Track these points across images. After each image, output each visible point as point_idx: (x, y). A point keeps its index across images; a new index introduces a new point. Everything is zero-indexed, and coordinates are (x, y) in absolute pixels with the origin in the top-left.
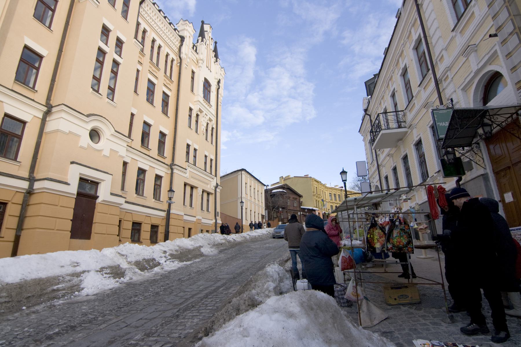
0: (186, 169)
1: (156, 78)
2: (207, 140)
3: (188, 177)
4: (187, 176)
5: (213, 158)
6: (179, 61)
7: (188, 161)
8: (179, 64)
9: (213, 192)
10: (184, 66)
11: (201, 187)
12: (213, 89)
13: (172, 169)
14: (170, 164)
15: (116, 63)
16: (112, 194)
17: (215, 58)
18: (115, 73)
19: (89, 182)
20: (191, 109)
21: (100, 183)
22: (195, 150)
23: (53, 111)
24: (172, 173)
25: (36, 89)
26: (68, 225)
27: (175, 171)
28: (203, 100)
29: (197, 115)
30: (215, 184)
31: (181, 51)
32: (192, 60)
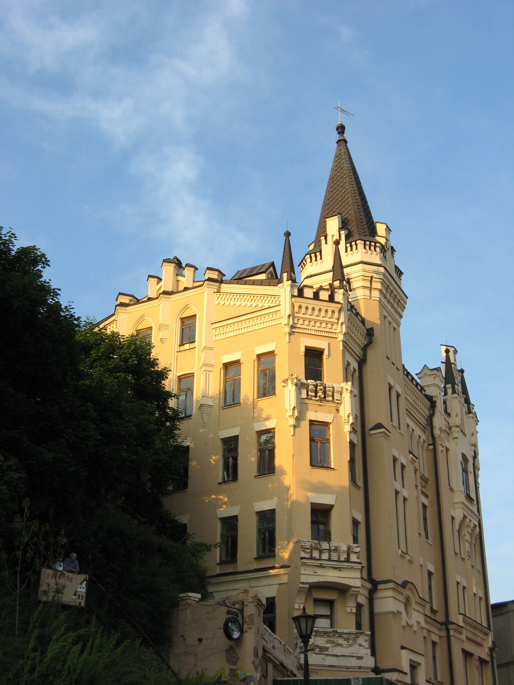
4: (463, 638)
5: (481, 594)
6: (431, 442)
8: (431, 447)
10: (440, 448)
13: (448, 630)
17: (466, 405)
21: (417, 667)
22: (464, 588)
23: (379, 588)
24: (448, 637)
27: (452, 633)
28: (465, 497)
29: (460, 524)
30: (490, 644)
31: (434, 425)
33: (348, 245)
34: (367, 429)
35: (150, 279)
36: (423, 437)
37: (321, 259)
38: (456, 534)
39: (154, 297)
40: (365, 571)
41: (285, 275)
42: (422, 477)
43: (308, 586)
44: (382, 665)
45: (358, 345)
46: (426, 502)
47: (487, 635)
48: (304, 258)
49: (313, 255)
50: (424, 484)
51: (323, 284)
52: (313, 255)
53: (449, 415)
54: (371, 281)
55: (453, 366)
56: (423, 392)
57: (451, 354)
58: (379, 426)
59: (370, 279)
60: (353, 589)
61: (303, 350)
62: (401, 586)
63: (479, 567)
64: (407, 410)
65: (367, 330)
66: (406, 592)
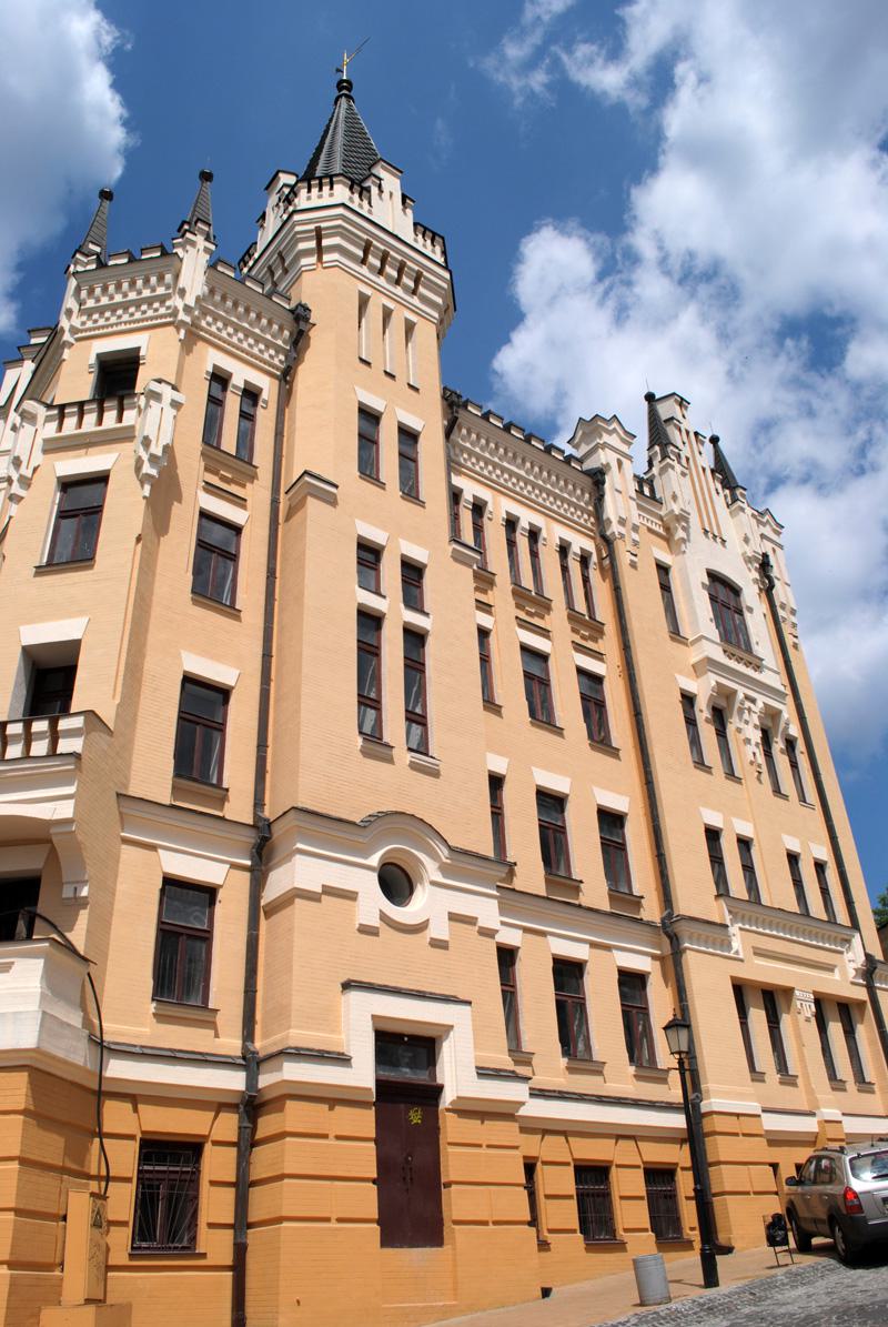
1: (545, 633)
2: (777, 791)
3: (741, 956)
4: (737, 952)
5: (824, 853)
8: (607, 562)
9: (861, 994)
10: (624, 558)
11: (804, 983)
12: (751, 595)
13: (674, 939)
14: (663, 920)
16: (484, 1073)
17: (727, 492)
18: (415, 667)
19: (406, 1039)
20: (688, 700)
22: (744, 844)
25: (225, 785)
26: (367, 1200)
28: (725, 651)
32: (650, 530)
36: (580, 543)
38: (707, 732)
47: (848, 941)
54: (319, 237)
61: (93, 360)
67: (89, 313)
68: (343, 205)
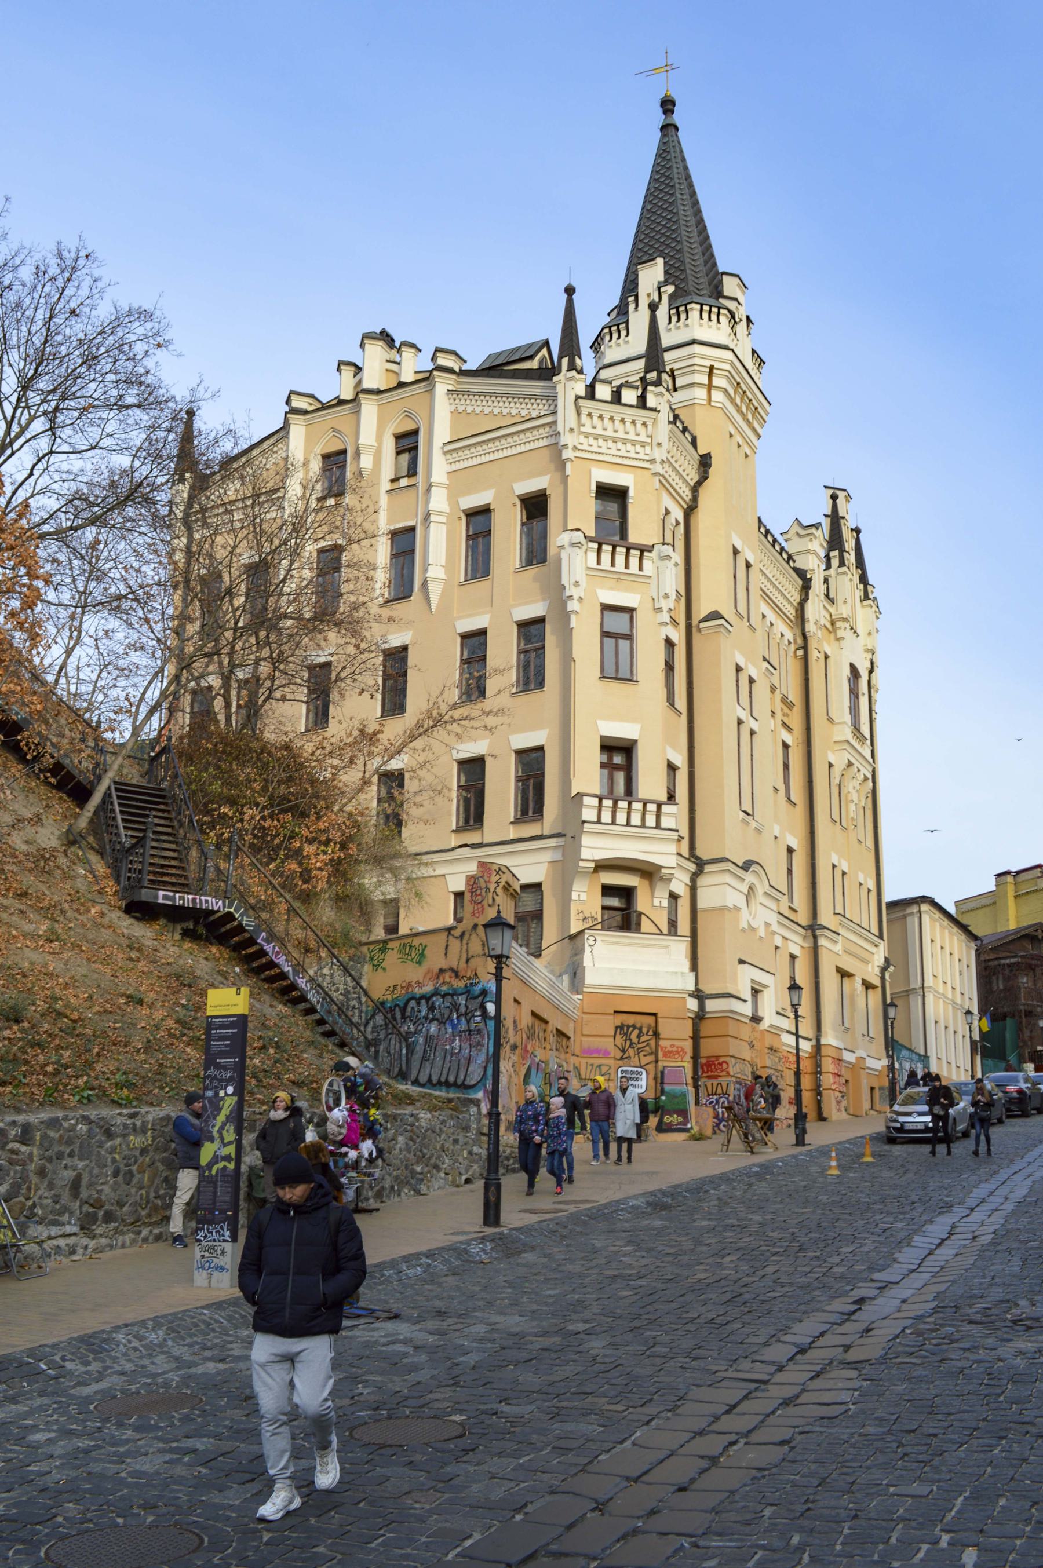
0: (838, 934)
5: (871, 884)
6: (800, 641)
7: (835, 914)
8: (800, 653)
10: (814, 655)
15: (752, 733)
17: (861, 586)
20: (831, 765)
24: (815, 950)
27: (822, 942)
33: (673, 311)
34: (695, 622)
35: (342, 367)
36: (789, 635)
37: (628, 335)
38: (835, 791)
39: (349, 398)
40: (685, 844)
41: (565, 361)
42: (784, 700)
43: (592, 865)
44: (707, 988)
45: (685, 481)
46: (789, 740)
48: (599, 334)
49: (614, 328)
50: (786, 710)
51: (631, 379)
52: (614, 328)
53: (832, 601)
55: (842, 521)
56: (791, 563)
57: (841, 502)
58: (715, 615)
59: (708, 370)
60: (664, 871)
61: (594, 488)
62: (741, 868)
63: (870, 843)
64: (762, 590)
65: (701, 456)
66: (749, 878)
67: (587, 436)
68: (732, 350)
